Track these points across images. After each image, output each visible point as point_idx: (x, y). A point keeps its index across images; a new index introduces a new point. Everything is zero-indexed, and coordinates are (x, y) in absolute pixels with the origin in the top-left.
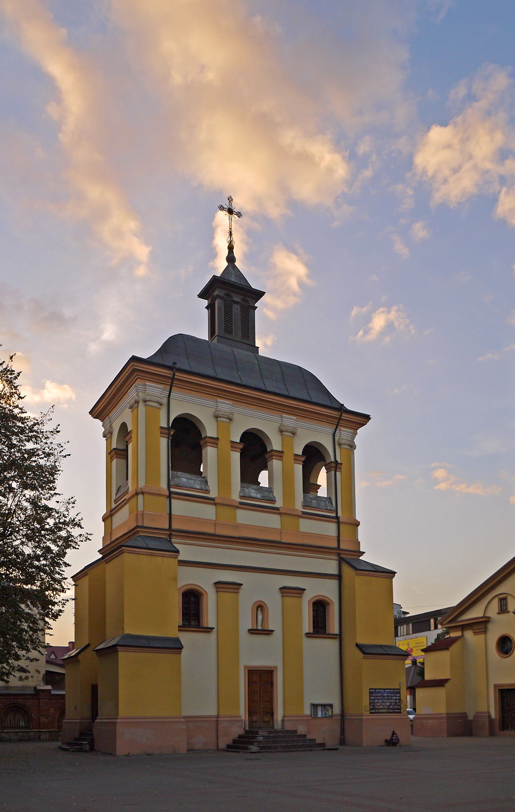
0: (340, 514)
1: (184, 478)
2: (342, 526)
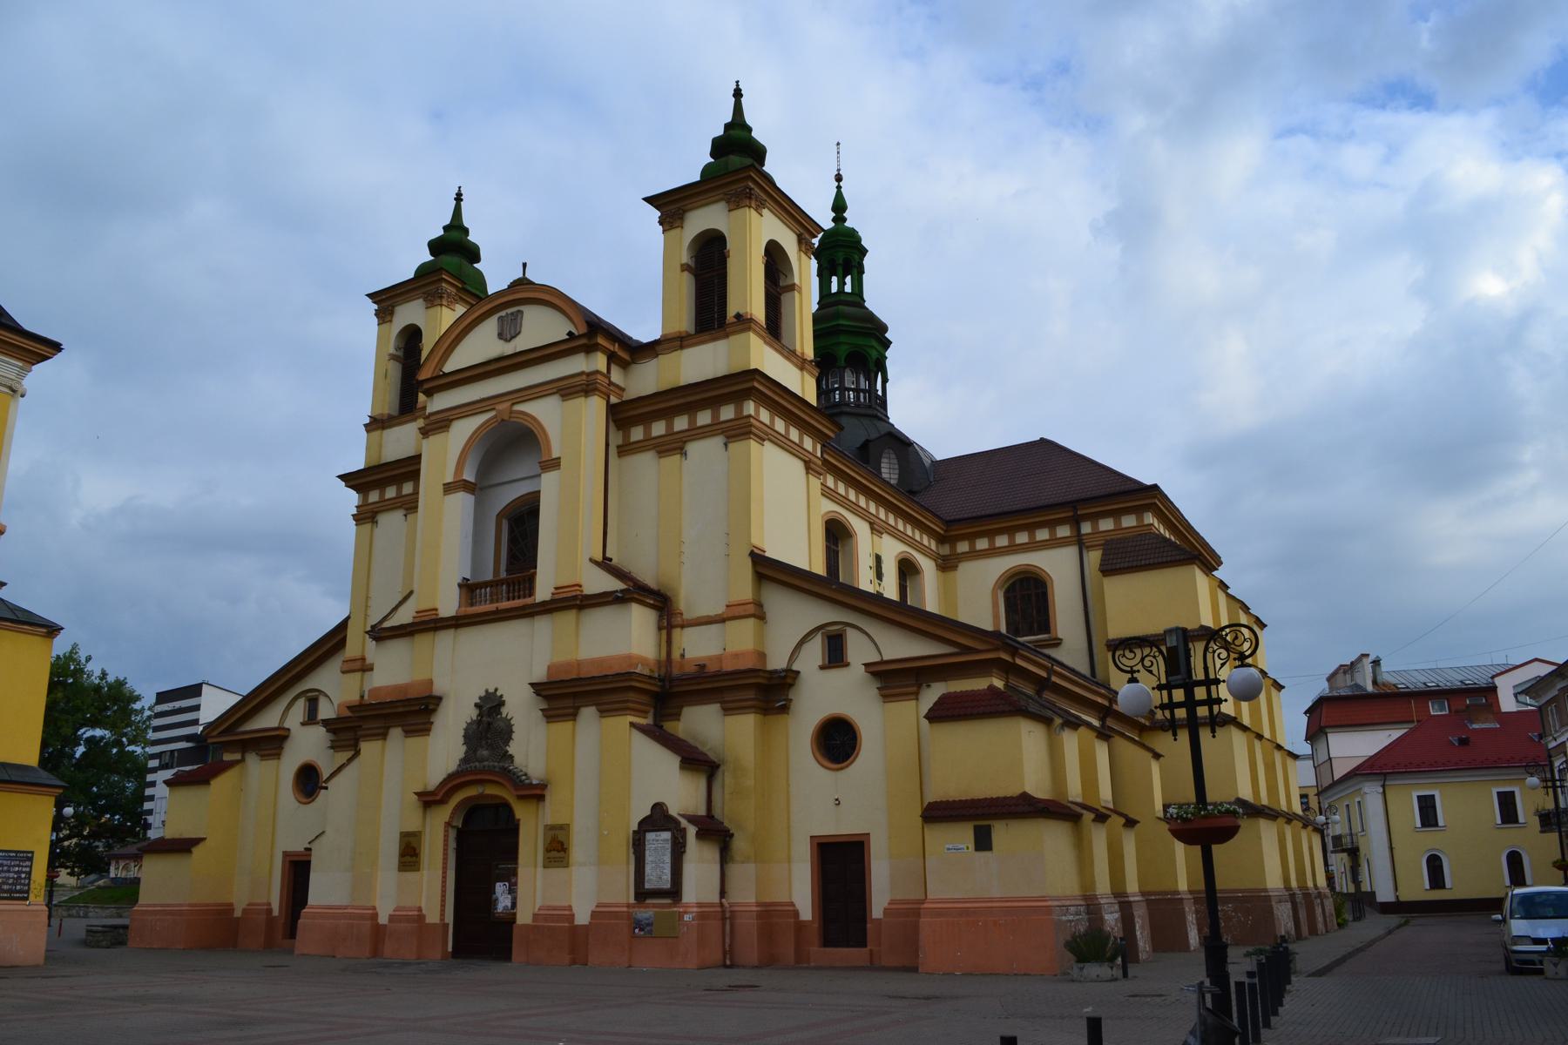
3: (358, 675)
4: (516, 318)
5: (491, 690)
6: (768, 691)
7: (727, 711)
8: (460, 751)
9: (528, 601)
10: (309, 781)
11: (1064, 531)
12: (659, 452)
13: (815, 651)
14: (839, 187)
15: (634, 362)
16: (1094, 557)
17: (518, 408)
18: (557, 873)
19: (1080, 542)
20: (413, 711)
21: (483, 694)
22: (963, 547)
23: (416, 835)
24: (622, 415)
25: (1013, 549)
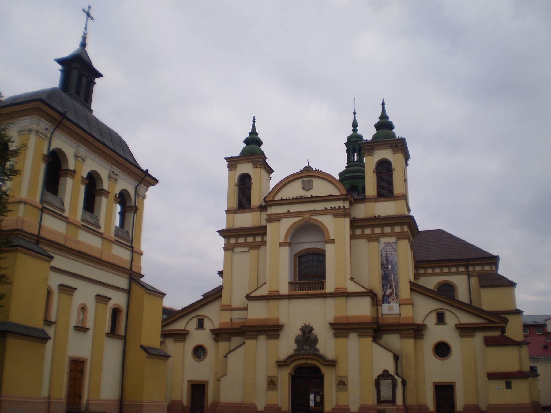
0: (133, 245)
1: (50, 197)
2: (134, 254)
3: (229, 312)
5: (307, 324)
6: (417, 331)
7: (402, 337)
8: (295, 346)
9: (322, 291)
10: (199, 352)
11: (462, 269)
12: (368, 240)
14: (355, 117)
15: (355, 203)
16: (474, 281)
17: (312, 217)
19: (469, 274)
20: (272, 330)
21: (303, 325)
22: (422, 271)
23: (276, 377)
24: (355, 224)
25: (442, 274)
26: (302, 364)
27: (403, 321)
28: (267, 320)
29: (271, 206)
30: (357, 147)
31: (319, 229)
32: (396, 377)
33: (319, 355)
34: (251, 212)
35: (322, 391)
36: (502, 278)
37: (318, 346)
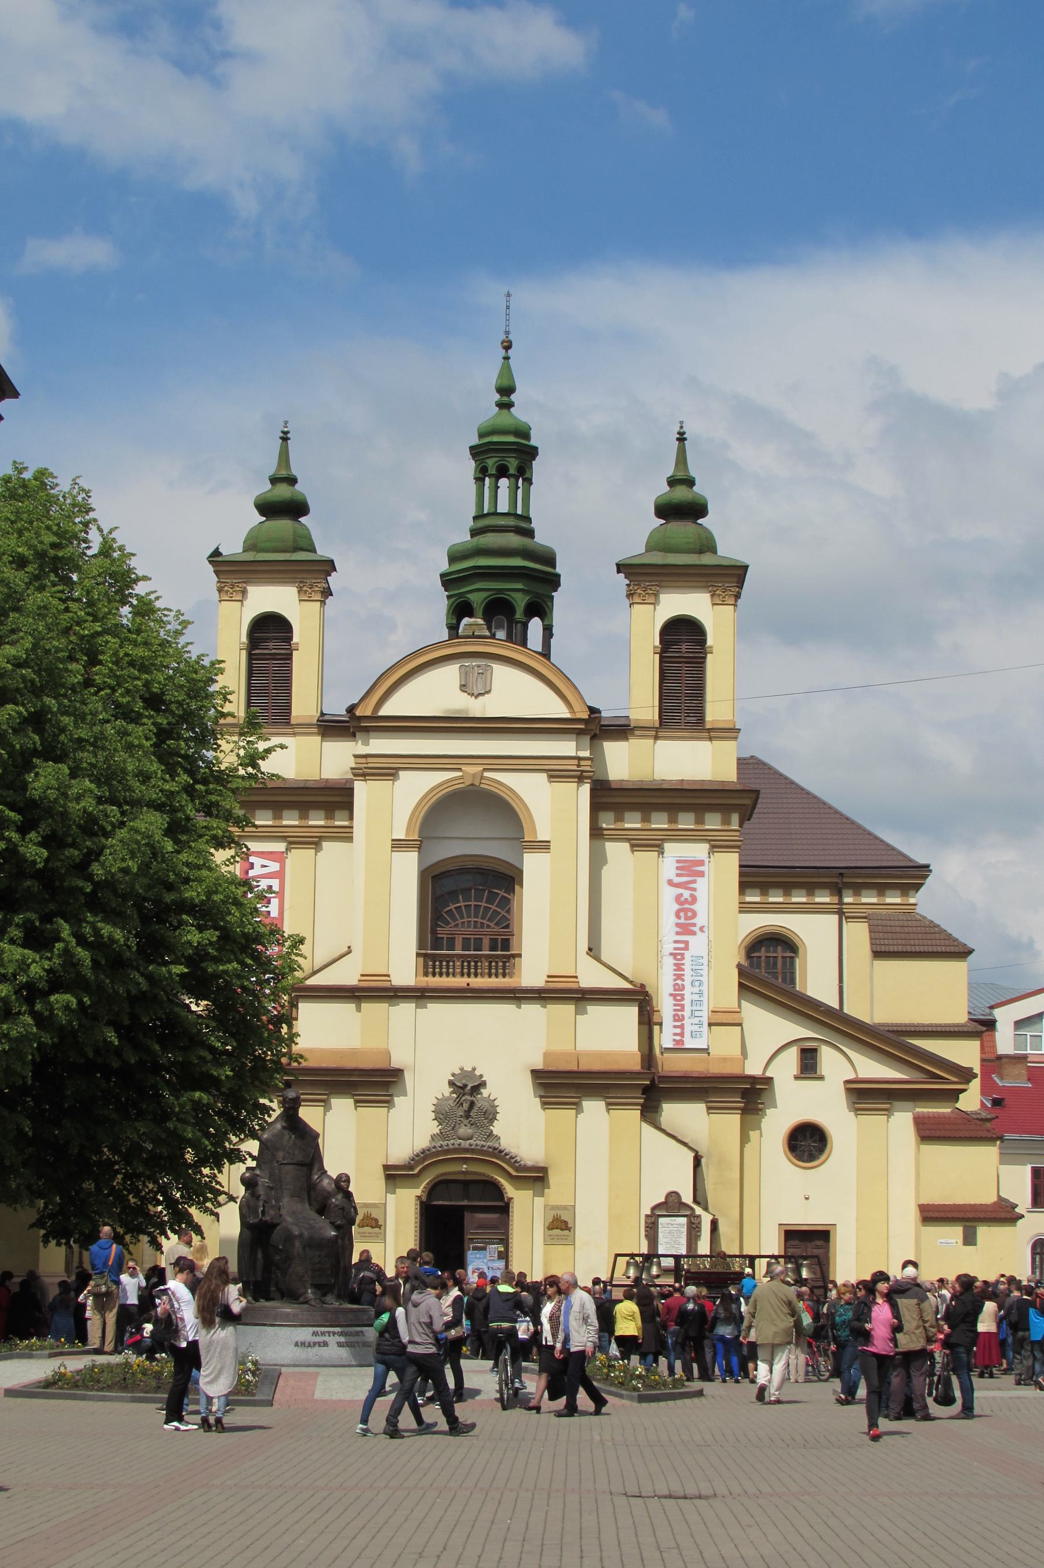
4: (485, 674)
8: (434, 1128)
11: (823, 898)
13: (791, 1059)
14: (507, 358)
16: (858, 934)
17: (486, 774)
18: (560, 1251)
20: (373, 1083)
21: (458, 1072)
26: (445, 1174)
27: (715, 1069)
28: (354, 1053)
29: (367, 730)
30: (513, 464)
31: (502, 810)
32: (698, 1210)
33: (501, 1151)
34: (295, 734)
35: (505, 1242)
36: (932, 929)
37: (497, 1128)
